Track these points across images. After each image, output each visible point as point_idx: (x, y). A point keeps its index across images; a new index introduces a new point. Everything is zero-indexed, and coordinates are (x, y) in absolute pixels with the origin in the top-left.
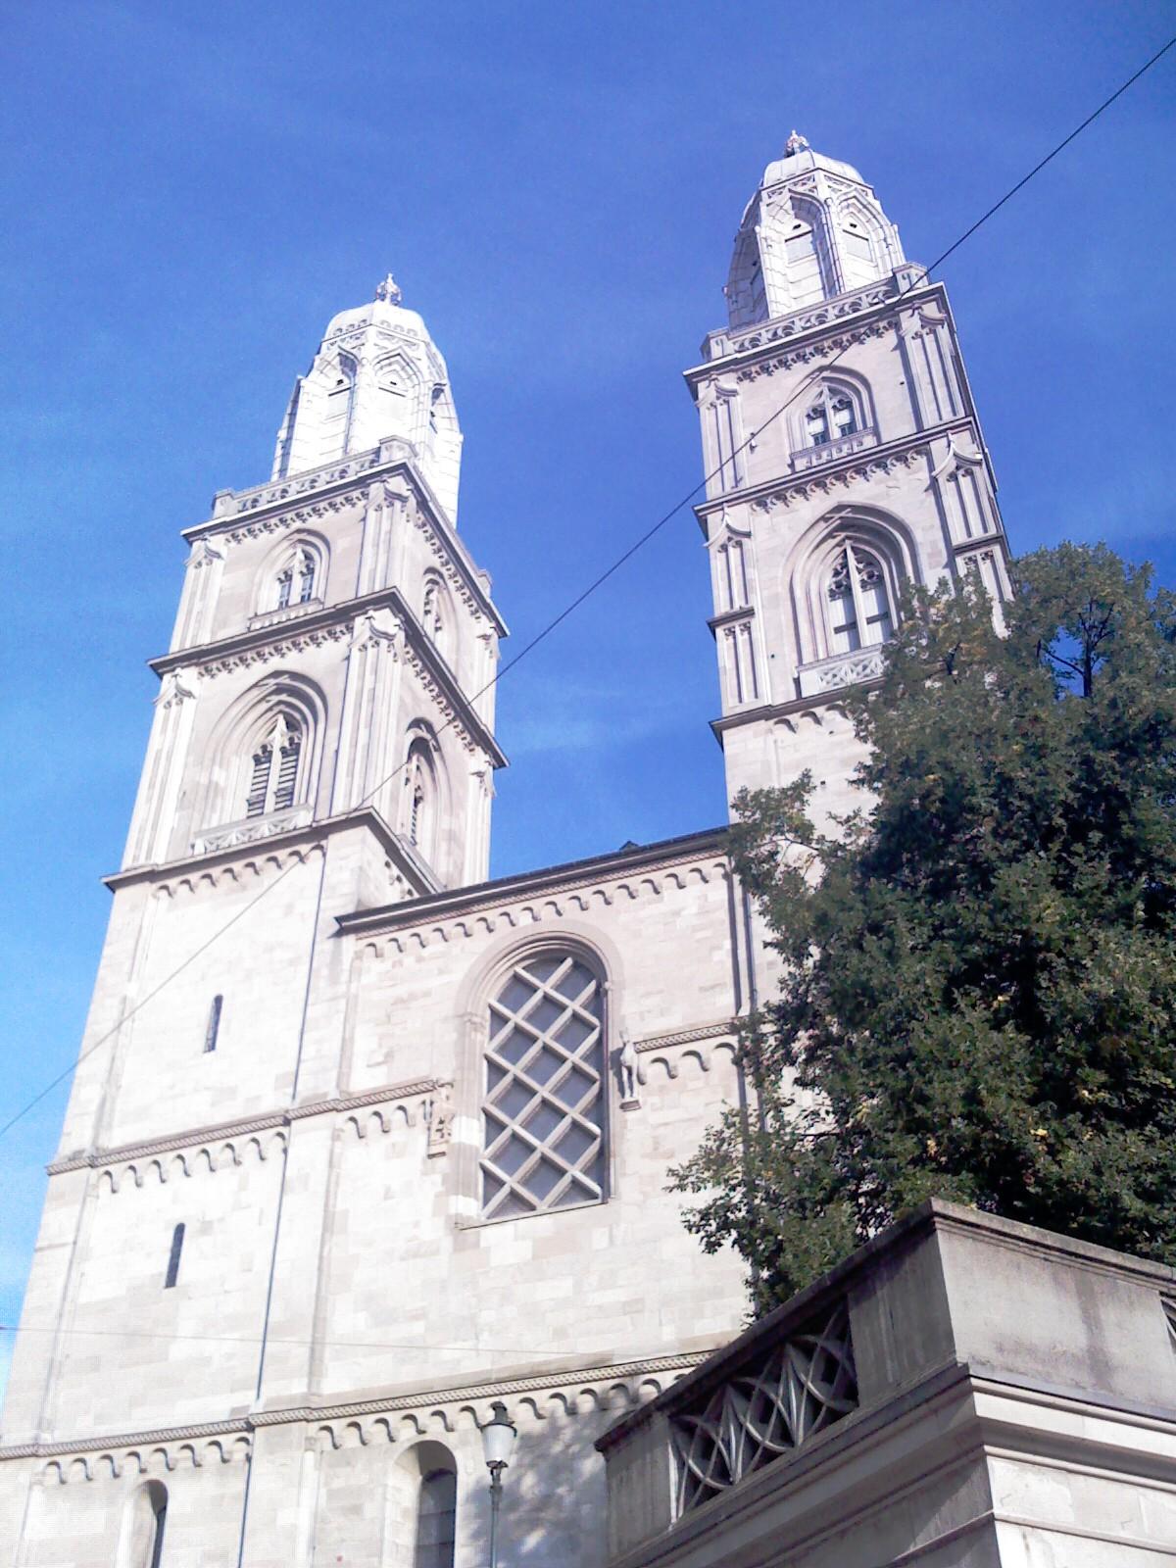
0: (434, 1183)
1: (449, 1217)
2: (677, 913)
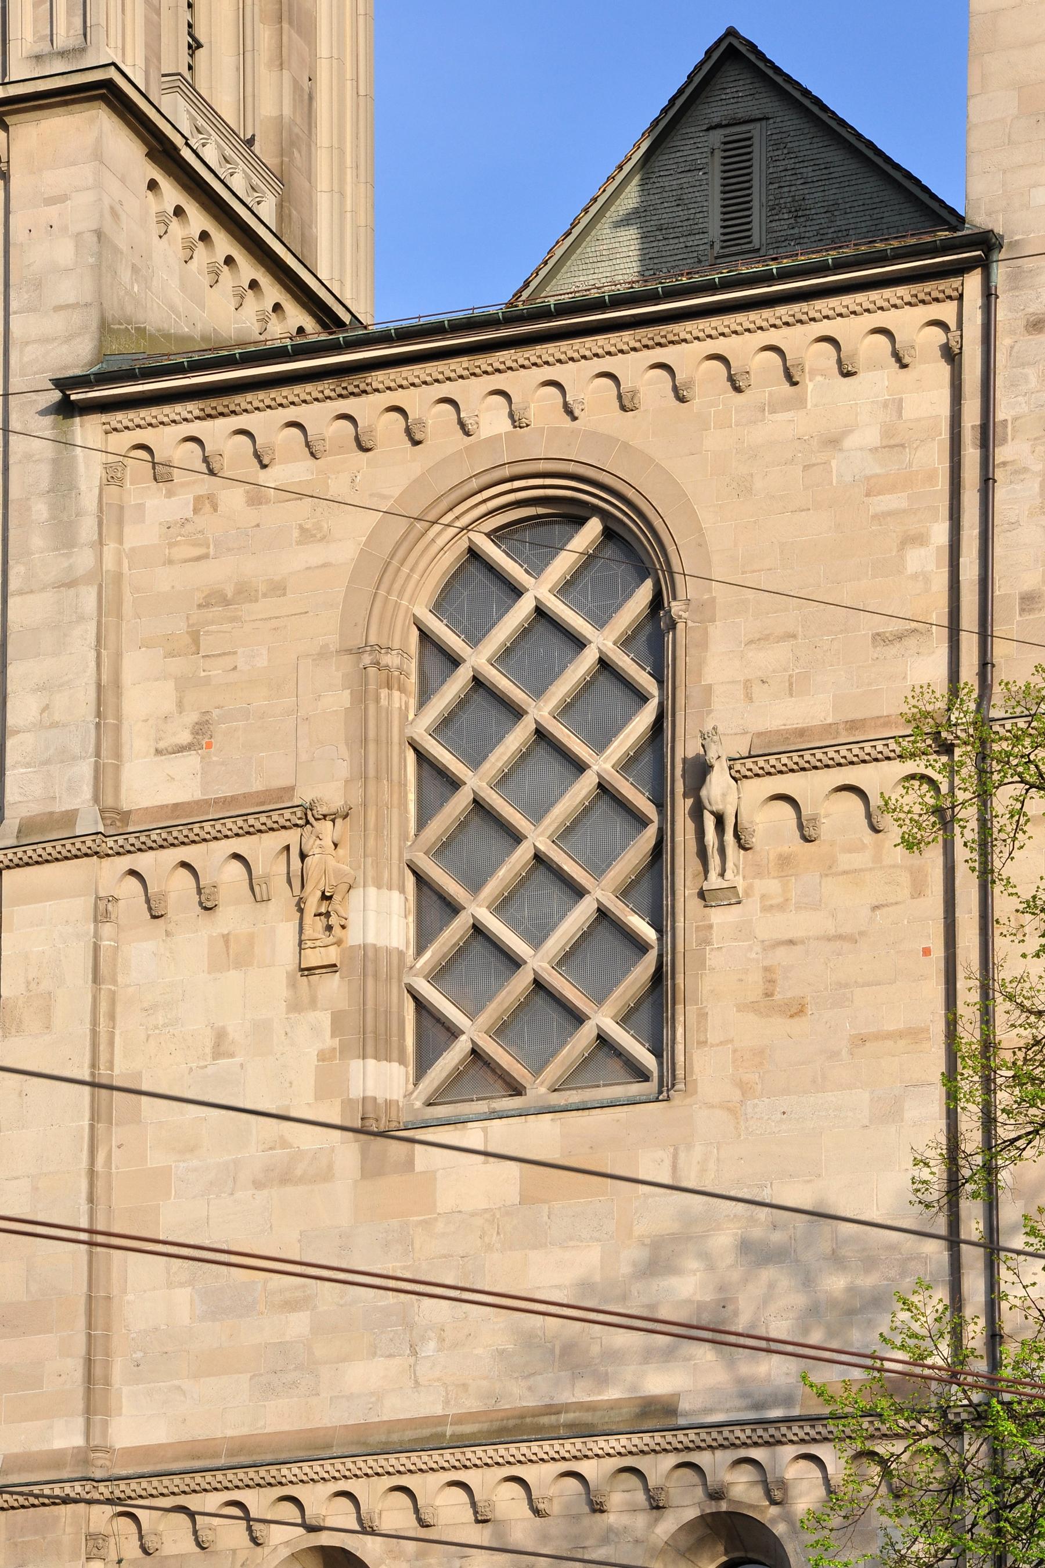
0: (313, 1033)
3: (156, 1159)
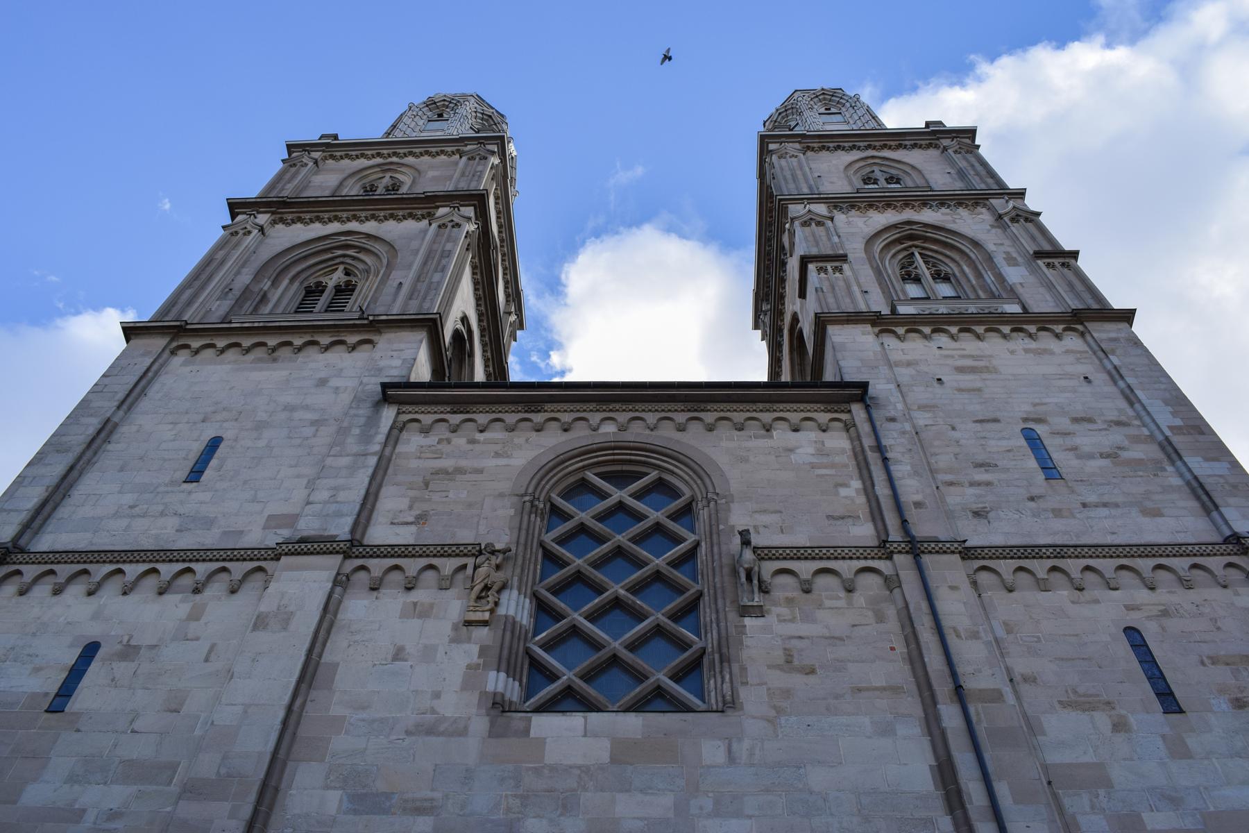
0: (468, 653)
1: (484, 694)
2: (791, 450)
3: (336, 710)
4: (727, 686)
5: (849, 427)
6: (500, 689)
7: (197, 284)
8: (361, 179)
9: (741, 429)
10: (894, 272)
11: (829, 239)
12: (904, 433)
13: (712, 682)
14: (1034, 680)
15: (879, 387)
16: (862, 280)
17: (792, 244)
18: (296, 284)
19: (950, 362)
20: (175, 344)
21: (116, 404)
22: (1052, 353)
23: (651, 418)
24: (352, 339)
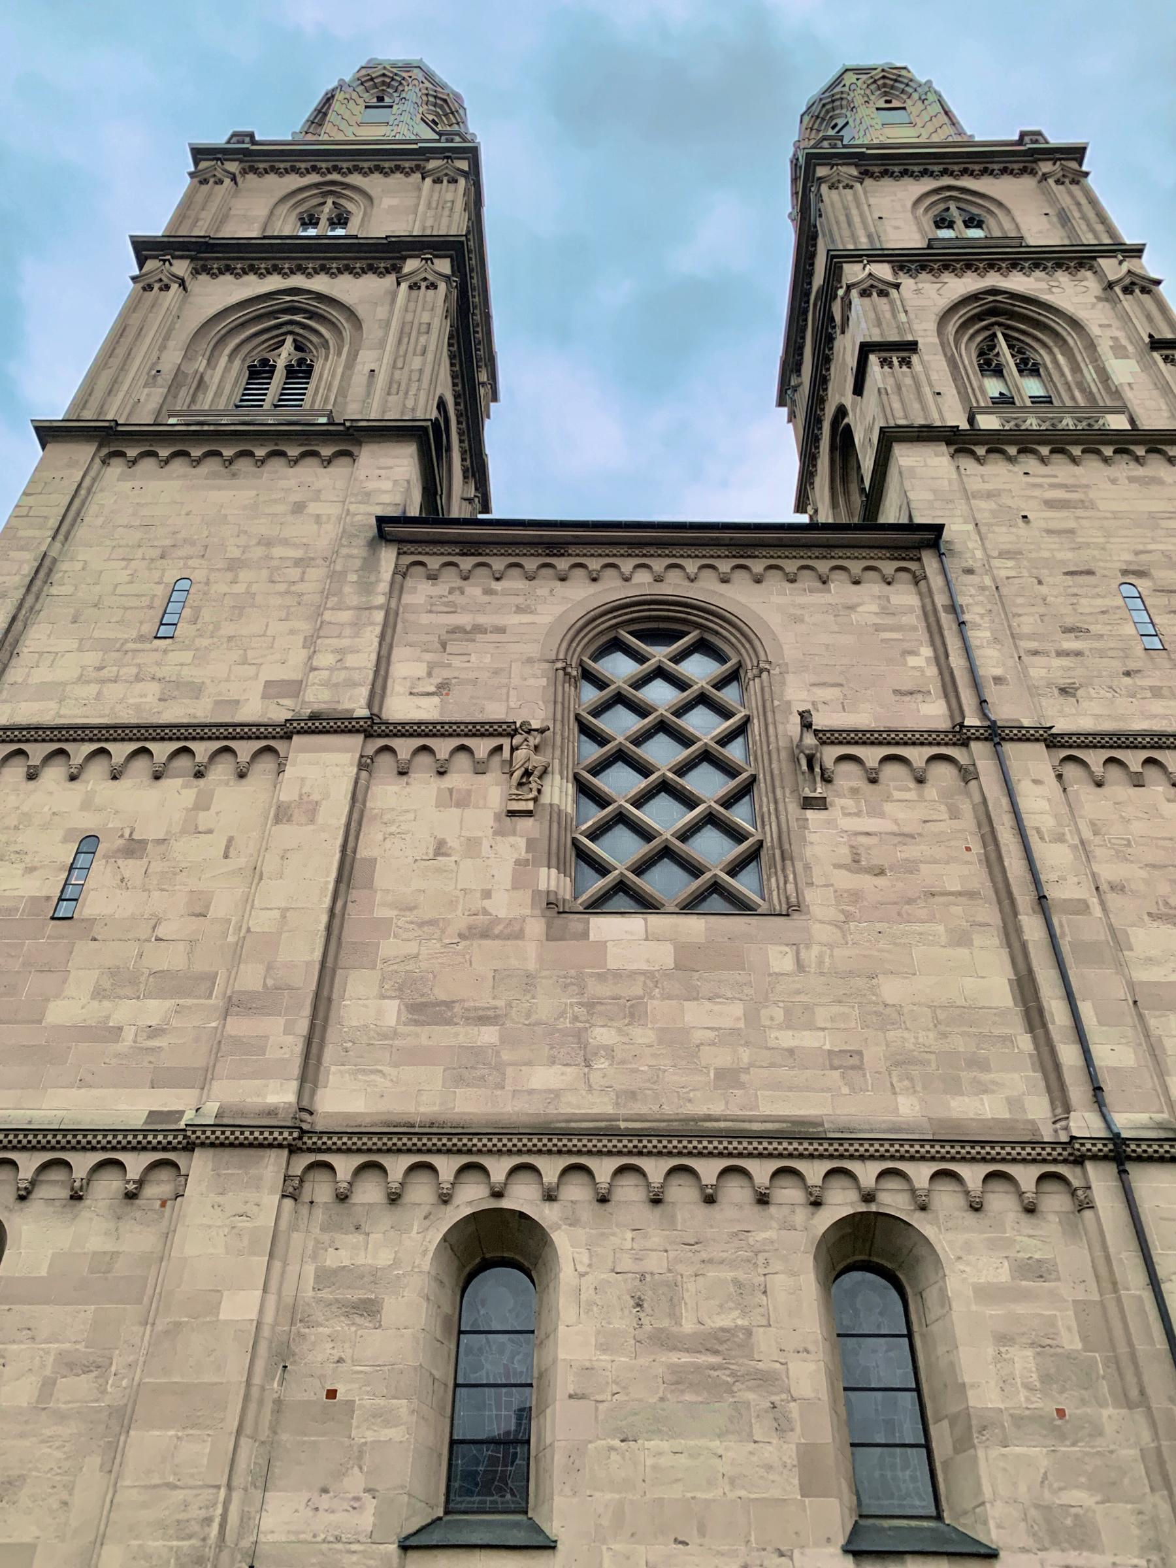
0: (514, 846)
1: (536, 893)
3: (381, 913)
4: (790, 887)
5: (918, 579)
6: (553, 888)
7: (115, 362)
8: (296, 205)
9: (793, 581)
10: (971, 362)
11: (894, 316)
12: (983, 588)
13: (773, 880)
14: (1123, 889)
15: (954, 527)
16: (934, 376)
17: (846, 320)
18: (237, 363)
19: (1037, 493)
20: (104, 451)
21: (51, 533)
22: (1159, 482)
23: (691, 566)
24: (326, 451)
